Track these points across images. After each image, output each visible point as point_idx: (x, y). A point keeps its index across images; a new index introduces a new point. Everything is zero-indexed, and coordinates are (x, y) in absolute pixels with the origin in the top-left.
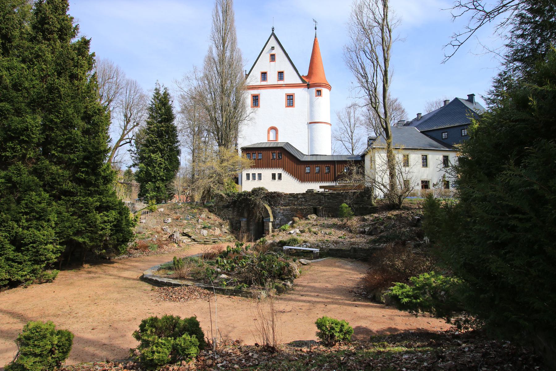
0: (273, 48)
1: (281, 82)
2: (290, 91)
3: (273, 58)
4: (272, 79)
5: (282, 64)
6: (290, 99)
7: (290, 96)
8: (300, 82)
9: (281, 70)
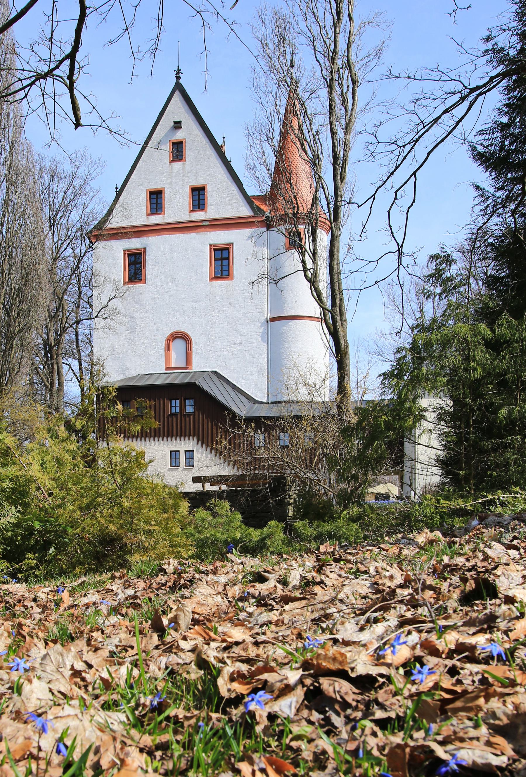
0: (177, 125)
1: (199, 216)
2: (221, 237)
4: (177, 208)
6: (222, 259)
7: (222, 250)
8: (245, 211)
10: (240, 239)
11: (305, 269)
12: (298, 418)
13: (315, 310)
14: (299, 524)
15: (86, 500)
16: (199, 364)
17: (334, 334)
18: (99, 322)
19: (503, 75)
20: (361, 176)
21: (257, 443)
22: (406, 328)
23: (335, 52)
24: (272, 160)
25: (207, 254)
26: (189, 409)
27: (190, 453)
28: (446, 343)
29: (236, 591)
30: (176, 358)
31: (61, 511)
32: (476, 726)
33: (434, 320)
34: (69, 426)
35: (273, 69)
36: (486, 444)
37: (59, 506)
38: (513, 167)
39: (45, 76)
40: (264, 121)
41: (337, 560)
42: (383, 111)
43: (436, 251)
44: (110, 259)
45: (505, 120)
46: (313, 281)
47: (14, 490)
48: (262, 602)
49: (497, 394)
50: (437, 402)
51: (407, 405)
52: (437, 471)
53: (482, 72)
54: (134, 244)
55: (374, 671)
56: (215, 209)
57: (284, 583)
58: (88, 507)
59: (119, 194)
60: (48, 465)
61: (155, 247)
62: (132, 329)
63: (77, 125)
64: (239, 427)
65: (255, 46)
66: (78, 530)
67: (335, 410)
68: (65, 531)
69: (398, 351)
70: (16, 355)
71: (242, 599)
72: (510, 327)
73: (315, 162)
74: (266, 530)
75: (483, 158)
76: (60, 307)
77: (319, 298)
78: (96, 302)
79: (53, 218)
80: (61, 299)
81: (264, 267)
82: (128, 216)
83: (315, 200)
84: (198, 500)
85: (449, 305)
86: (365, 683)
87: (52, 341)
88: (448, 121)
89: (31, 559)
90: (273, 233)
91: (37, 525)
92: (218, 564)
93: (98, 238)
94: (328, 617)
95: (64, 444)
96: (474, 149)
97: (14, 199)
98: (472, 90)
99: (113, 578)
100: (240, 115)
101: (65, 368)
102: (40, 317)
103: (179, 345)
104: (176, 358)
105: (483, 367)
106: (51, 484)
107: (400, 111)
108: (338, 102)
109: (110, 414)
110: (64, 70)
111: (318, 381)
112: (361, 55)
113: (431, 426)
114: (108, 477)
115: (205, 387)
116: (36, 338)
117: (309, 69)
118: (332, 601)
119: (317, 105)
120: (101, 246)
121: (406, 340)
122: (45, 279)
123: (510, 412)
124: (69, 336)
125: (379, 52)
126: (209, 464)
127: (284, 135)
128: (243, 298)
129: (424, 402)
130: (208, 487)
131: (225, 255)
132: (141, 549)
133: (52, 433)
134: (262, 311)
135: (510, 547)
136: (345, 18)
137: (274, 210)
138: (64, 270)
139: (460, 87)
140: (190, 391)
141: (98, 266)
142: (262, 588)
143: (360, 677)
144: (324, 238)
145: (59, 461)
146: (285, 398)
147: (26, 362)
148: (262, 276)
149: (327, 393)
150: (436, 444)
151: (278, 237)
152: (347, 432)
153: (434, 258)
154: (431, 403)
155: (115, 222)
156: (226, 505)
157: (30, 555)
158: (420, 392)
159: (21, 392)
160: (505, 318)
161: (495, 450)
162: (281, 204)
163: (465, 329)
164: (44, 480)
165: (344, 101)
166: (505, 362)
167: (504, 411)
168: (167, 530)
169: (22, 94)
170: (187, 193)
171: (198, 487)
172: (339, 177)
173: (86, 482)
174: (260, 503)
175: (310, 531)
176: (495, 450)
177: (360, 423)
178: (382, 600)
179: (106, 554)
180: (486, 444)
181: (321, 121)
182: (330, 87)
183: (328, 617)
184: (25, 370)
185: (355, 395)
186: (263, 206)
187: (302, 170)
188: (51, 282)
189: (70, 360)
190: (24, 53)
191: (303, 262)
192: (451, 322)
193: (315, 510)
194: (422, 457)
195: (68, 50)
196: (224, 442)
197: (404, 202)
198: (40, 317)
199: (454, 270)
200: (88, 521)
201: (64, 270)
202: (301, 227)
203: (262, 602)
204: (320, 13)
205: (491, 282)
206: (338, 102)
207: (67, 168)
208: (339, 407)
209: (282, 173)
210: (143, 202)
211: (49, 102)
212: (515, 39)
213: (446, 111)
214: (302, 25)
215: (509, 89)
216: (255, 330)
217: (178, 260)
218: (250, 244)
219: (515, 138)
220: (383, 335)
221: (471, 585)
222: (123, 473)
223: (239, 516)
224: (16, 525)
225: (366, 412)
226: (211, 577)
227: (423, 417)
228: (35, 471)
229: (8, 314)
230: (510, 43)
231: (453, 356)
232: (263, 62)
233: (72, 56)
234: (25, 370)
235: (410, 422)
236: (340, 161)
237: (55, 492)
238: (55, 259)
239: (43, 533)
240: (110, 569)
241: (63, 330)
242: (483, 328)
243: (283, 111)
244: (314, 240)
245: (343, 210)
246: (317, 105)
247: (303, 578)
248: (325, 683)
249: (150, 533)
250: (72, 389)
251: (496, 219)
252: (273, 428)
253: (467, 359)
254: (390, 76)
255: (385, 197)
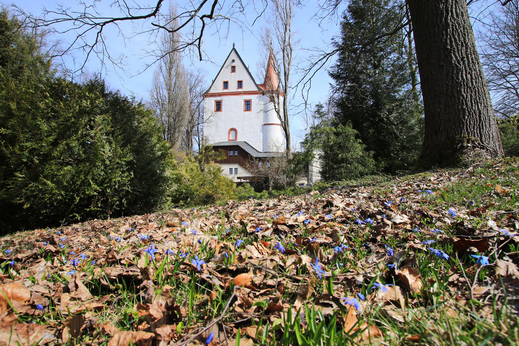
3: (233, 69)
5: (241, 74)
6: (248, 104)
8: (255, 89)
9: (240, 80)
10: (254, 98)
11: (275, 108)
12: (274, 157)
13: (279, 122)
14: (273, 191)
15: (201, 183)
16: (240, 139)
17: (285, 130)
18: (205, 124)
19: (337, 50)
20: (293, 79)
21: (259, 166)
22: (308, 128)
23: (285, 40)
24: (265, 73)
25: (243, 103)
26: (236, 154)
27: (236, 169)
28: (322, 133)
29: (252, 208)
30: (232, 137)
31: (192, 186)
32: (322, 235)
33: (317, 126)
34: (196, 158)
35: (265, 45)
36: (335, 166)
37: (192, 185)
38: (341, 78)
39: (191, 44)
40: (262, 61)
41: (285, 199)
42: (300, 58)
43: (317, 104)
44: (210, 103)
45: (339, 64)
46: (278, 112)
47: (177, 179)
48: (261, 211)
49: (339, 150)
50: (319, 153)
51: (310, 153)
52: (319, 175)
53: (331, 48)
54: (218, 99)
55: (294, 223)
56: (245, 88)
57: (268, 206)
58: (202, 185)
59: (213, 82)
60: (188, 171)
61: (225, 100)
62: (217, 127)
63: (201, 60)
64: (253, 160)
65: (259, 38)
66: (198, 193)
67: (286, 155)
68: (193, 193)
69: (306, 135)
70: (177, 135)
71: (254, 210)
72: (342, 129)
73: (278, 74)
74: (262, 193)
75: (332, 75)
76: (192, 119)
77: (280, 118)
78: (205, 117)
79: (191, 89)
80: (193, 116)
81: (262, 107)
82: (217, 90)
83: (279, 86)
84: (239, 184)
85: (322, 121)
86: (291, 227)
87: (189, 130)
88: (320, 63)
89: (182, 202)
90: (265, 96)
91: (184, 191)
92: (246, 201)
93: (206, 96)
94: (281, 213)
95: (194, 164)
96: (329, 72)
97: (178, 83)
98: (328, 54)
99: (211, 206)
100: (255, 59)
101: (194, 140)
102: (185, 122)
103: (233, 132)
104: (232, 137)
105: (333, 141)
106: (189, 177)
107: (306, 60)
108: (286, 56)
109: (210, 154)
110: (197, 43)
111: (280, 145)
112: (293, 42)
113: (317, 160)
114: (209, 175)
115: (242, 147)
116: (184, 129)
117: (277, 46)
118: (283, 209)
119: (279, 56)
120: (207, 99)
121: (308, 131)
122: (188, 109)
123: (342, 156)
124: (195, 129)
125: (299, 41)
126: (243, 173)
127: (269, 66)
128: (255, 116)
129: (314, 153)
130: (242, 181)
131: (249, 103)
132: (219, 198)
133: (190, 161)
134: (261, 121)
135: (339, 195)
136: (288, 30)
137: (265, 89)
138: (194, 107)
139: (324, 53)
140: (237, 148)
141: (206, 106)
142: (261, 208)
143: (290, 225)
144: (281, 99)
145: (192, 169)
146: (269, 151)
147: (180, 137)
148: (261, 110)
149: (283, 149)
150: (319, 166)
151: (267, 98)
152: (289, 162)
153: (317, 106)
154: (317, 153)
155: (212, 91)
156: (249, 185)
157: (181, 201)
158: (313, 148)
159: (178, 147)
160: (340, 125)
161: (338, 168)
162: (268, 87)
163: (327, 129)
164: (187, 176)
165: (288, 56)
166: (340, 140)
167: (340, 156)
168: (228, 193)
169: (182, 50)
170: (237, 82)
171: (239, 181)
172: (286, 79)
173: (201, 176)
174: (260, 185)
175: (276, 194)
176: (338, 168)
177: (293, 159)
178: (299, 208)
179: (208, 200)
180: (335, 166)
181: (280, 62)
182: (283, 51)
183: (281, 213)
184: (180, 140)
185: (292, 150)
186: (261, 88)
187: (274, 77)
188: (190, 110)
189: (195, 137)
190: (184, 37)
191: (275, 106)
192: (323, 126)
193: (278, 187)
194: (314, 170)
195: (198, 37)
196: (248, 165)
197: (307, 87)
198: (185, 122)
199: (323, 110)
200: (202, 190)
201: (194, 107)
202: (274, 95)
203: (261, 211)
204: (280, 29)
205: (336, 114)
206: (286, 56)
207: (196, 73)
208: (287, 154)
209: (268, 78)
210: (222, 85)
211: (191, 52)
212: (341, 40)
213: (319, 60)
214: (274, 32)
215: (340, 55)
216: (258, 128)
217: (233, 104)
218: (257, 99)
219: (342, 69)
220: (301, 130)
221: (325, 203)
222: (214, 174)
223: (253, 189)
224: (177, 191)
225: (295, 155)
226: (244, 205)
227: (314, 157)
228: (183, 172)
229: (174, 121)
230: (340, 41)
231: (324, 137)
232: (261, 43)
233: (200, 38)
234: (180, 140)
235: (310, 158)
236: (287, 74)
237: (190, 180)
238: (191, 103)
239: (186, 194)
240: (210, 204)
241: (193, 127)
242: (333, 129)
243: (268, 58)
244: (278, 99)
245: (288, 89)
246: (279, 56)
247: (274, 204)
248: (280, 227)
249: (223, 194)
250: (196, 147)
251: (336, 94)
252: (265, 161)
253: (328, 139)
254: (302, 49)
255: (301, 86)
